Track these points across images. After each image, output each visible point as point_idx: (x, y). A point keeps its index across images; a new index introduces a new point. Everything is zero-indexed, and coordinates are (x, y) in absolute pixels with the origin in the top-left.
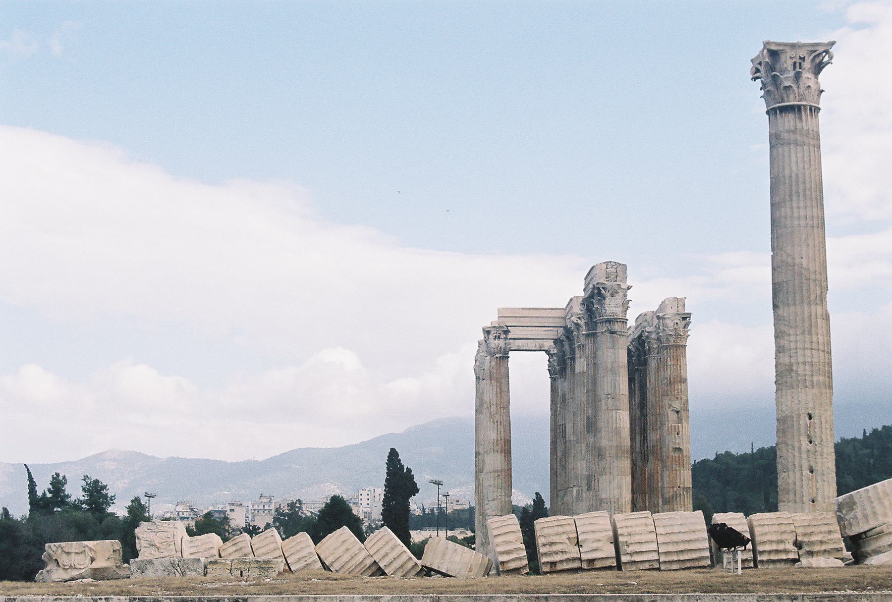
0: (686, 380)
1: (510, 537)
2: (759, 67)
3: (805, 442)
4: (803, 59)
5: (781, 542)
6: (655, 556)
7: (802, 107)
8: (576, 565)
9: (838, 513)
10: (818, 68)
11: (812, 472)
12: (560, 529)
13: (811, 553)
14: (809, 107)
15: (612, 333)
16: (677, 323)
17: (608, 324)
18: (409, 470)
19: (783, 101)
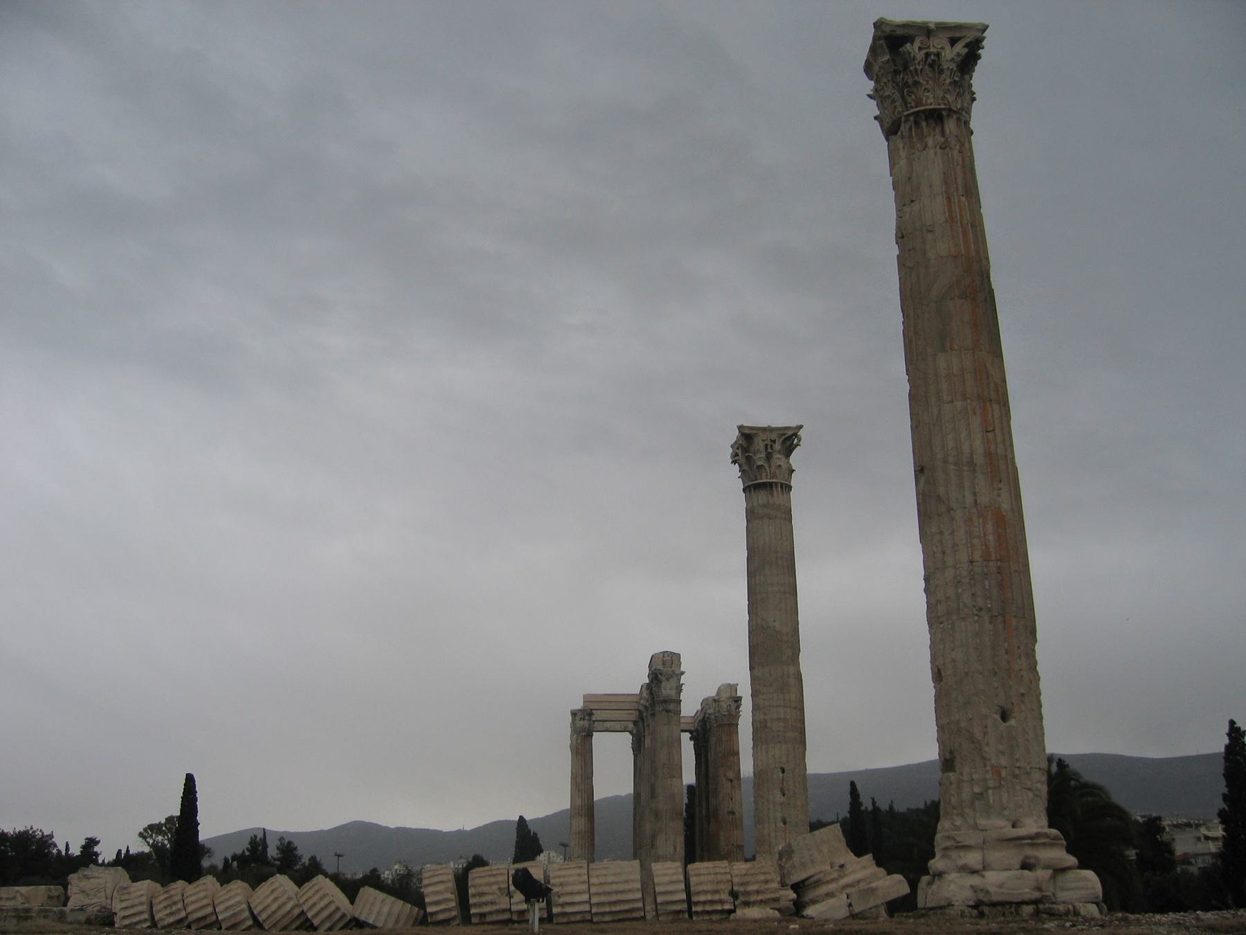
0: (738, 753)
1: (441, 887)
2: (737, 451)
3: (778, 793)
4: (774, 441)
5: (716, 892)
6: (586, 907)
7: (774, 484)
8: (506, 916)
9: (780, 862)
10: (788, 451)
11: (785, 823)
12: (492, 880)
13: (747, 904)
14: (779, 485)
15: (668, 711)
16: (730, 705)
17: (664, 704)
18: (535, 834)
19: (756, 480)
